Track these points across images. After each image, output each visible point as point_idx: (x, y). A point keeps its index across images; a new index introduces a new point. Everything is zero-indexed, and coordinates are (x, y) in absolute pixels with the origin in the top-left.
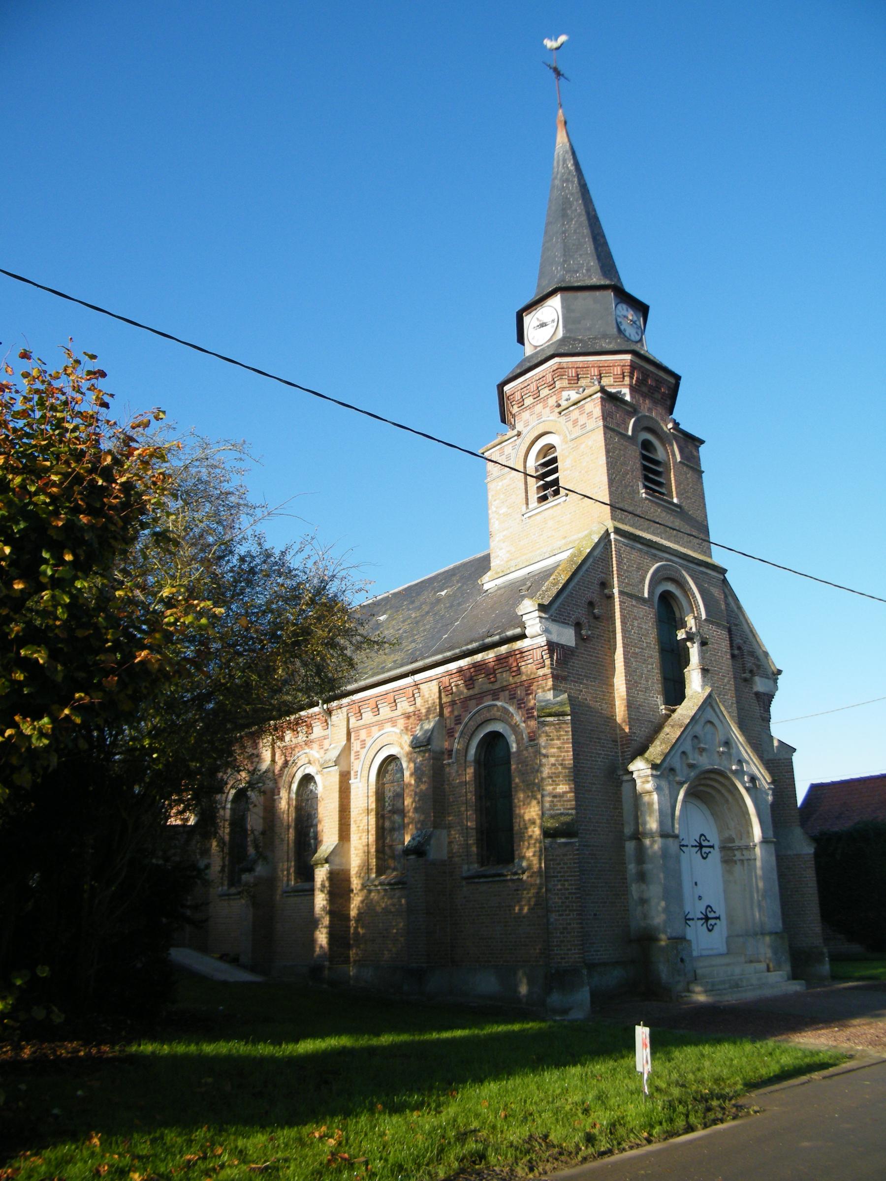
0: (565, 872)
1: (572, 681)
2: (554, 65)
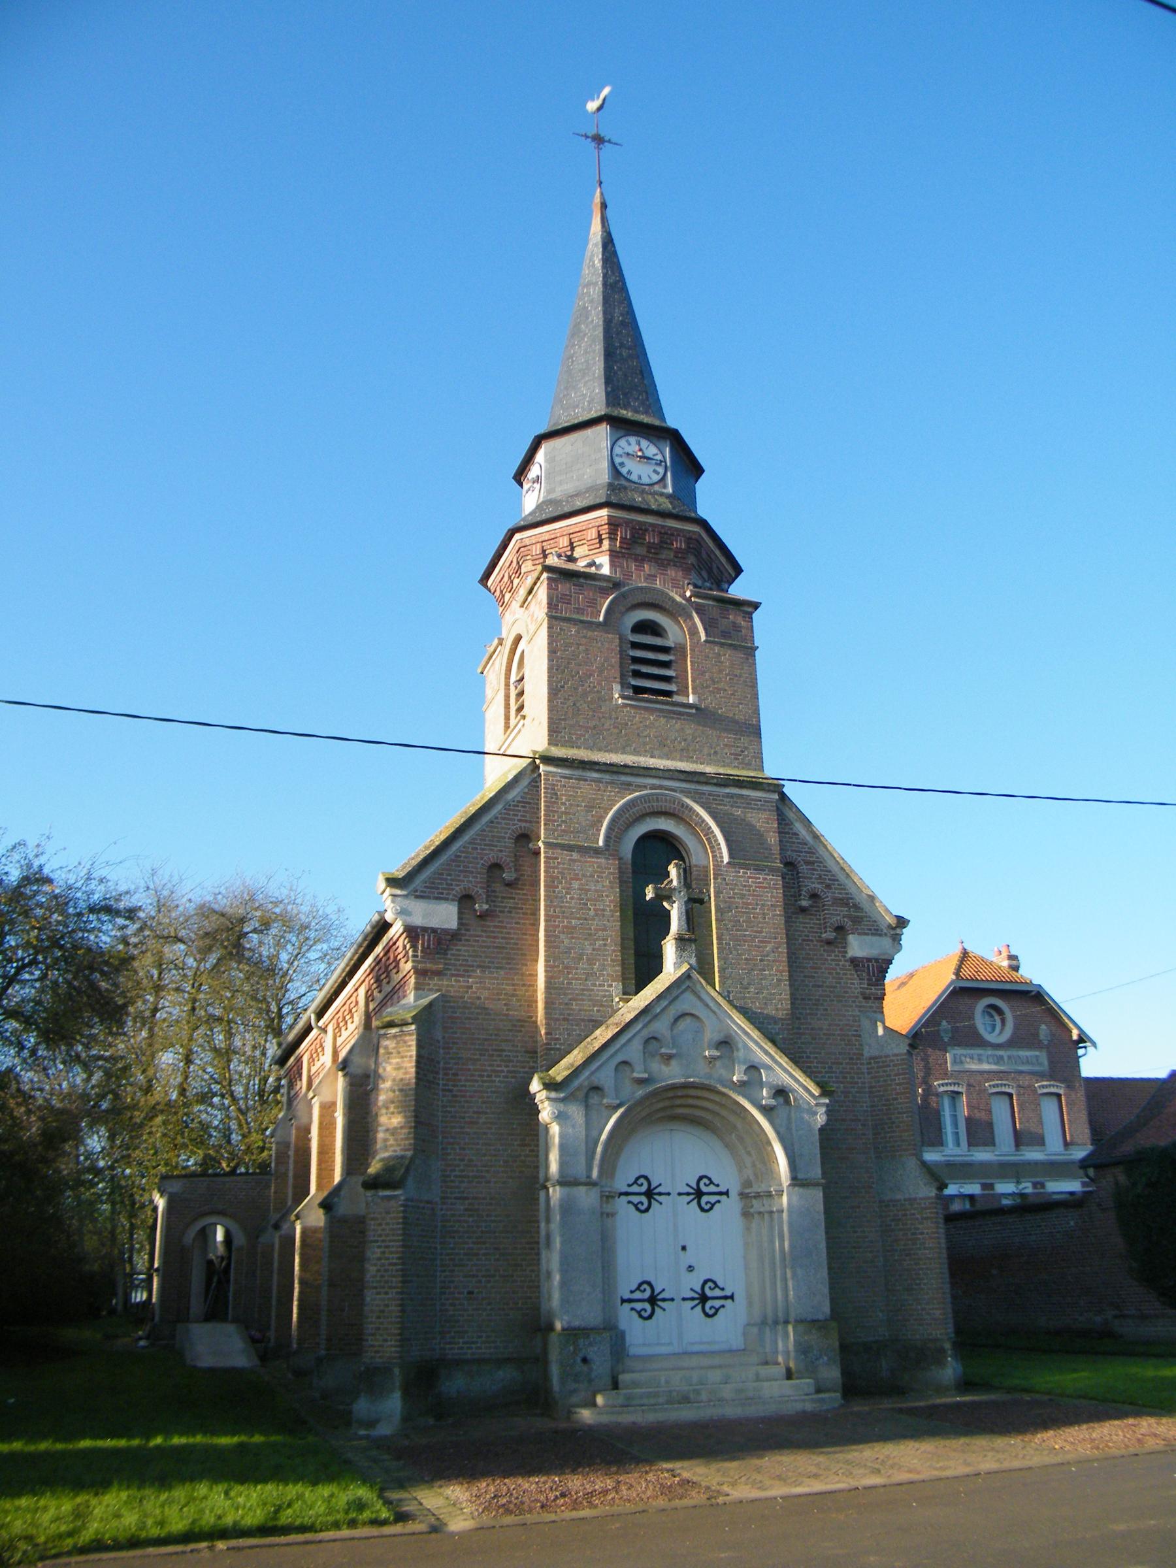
0: (387, 1235)
1: (453, 975)
2: (592, 131)
